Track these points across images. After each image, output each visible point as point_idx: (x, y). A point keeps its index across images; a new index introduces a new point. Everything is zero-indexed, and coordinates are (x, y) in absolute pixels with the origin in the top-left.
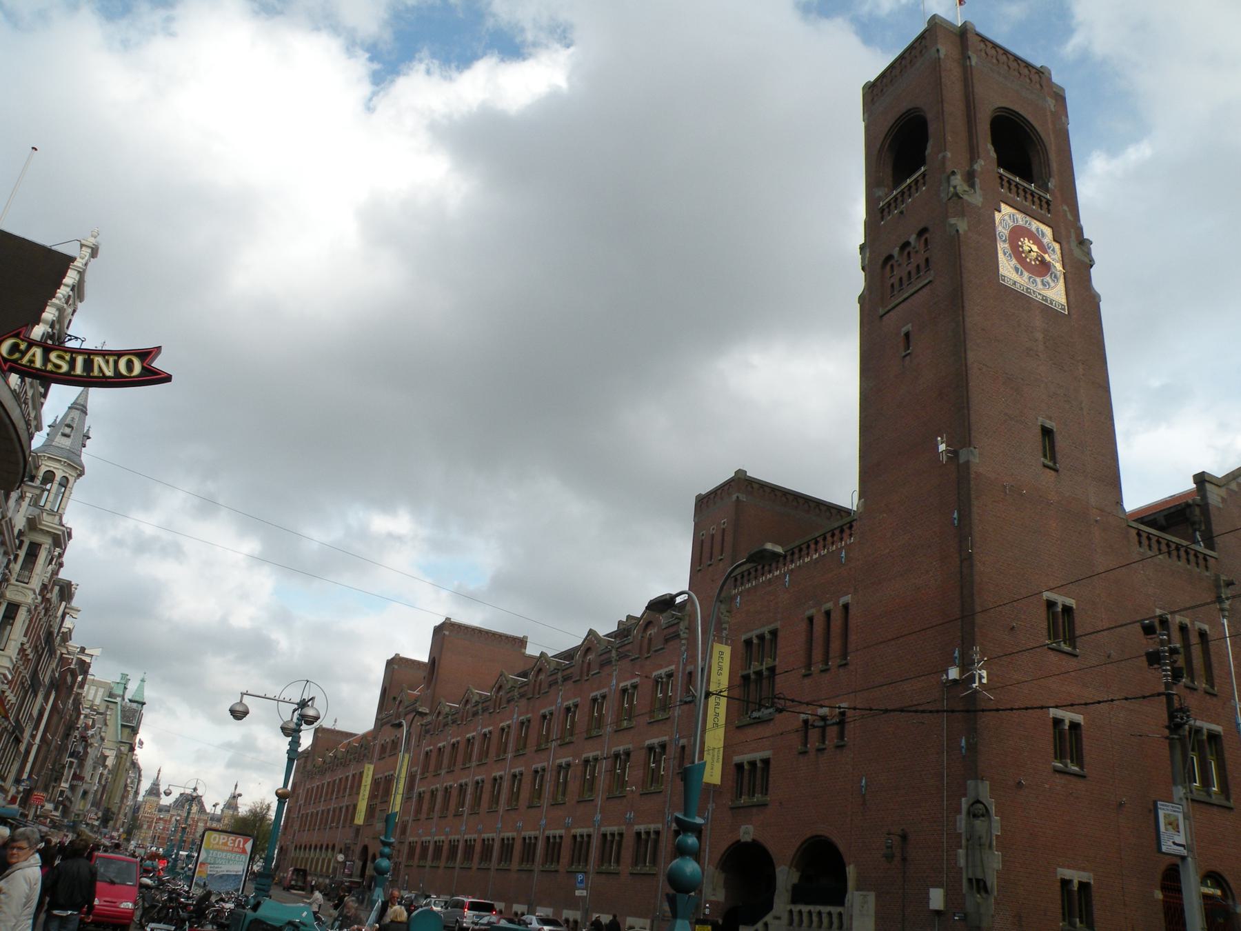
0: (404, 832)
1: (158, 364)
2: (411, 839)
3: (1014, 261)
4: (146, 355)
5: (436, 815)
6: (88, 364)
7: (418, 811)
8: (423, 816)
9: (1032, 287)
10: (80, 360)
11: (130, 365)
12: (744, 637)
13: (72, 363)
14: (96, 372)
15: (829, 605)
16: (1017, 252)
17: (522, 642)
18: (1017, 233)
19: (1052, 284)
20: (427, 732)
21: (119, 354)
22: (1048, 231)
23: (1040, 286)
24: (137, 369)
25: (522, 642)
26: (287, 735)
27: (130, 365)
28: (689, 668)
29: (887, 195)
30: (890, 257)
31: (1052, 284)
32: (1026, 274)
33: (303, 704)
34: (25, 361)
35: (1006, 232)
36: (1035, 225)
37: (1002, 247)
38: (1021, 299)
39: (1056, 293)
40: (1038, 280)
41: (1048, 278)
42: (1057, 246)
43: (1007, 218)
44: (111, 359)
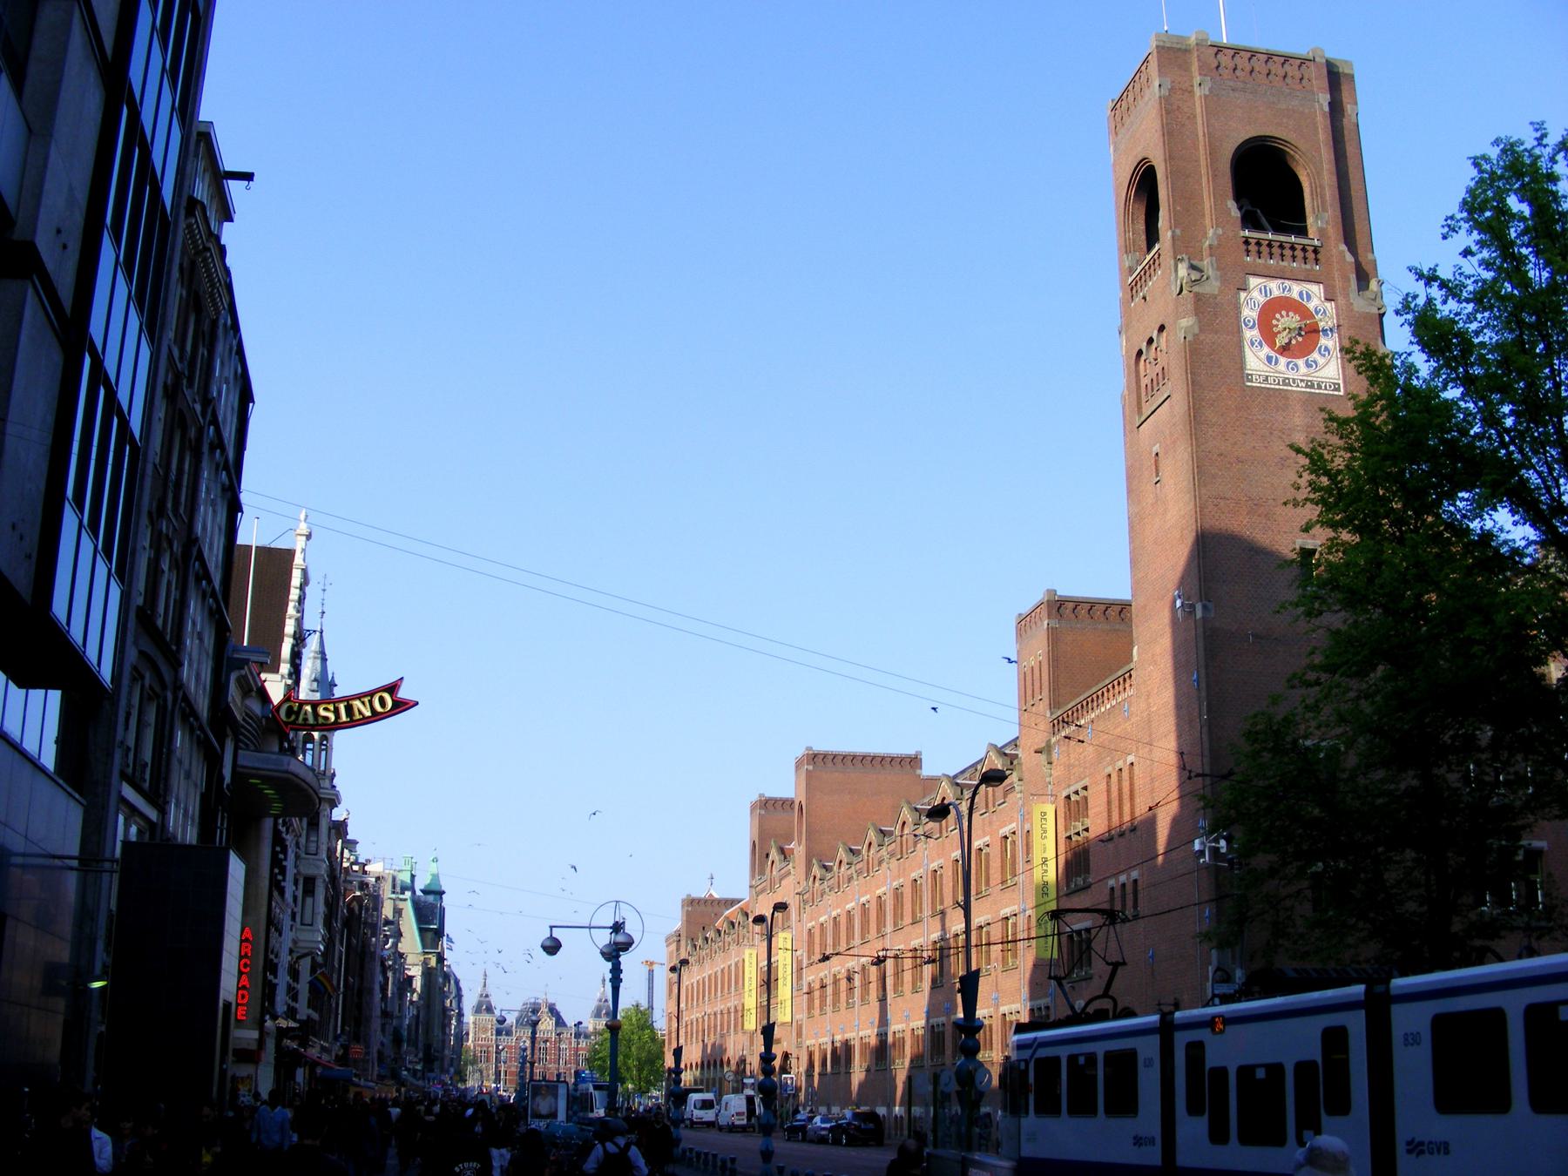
0: (799, 1035)
1: (403, 694)
2: (808, 1043)
3: (1266, 350)
4: (392, 689)
5: (829, 1009)
6: (349, 709)
7: (810, 1007)
8: (817, 1012)
9: (1291, 375)
10: (342, 707)
11: (382, 702)
12: (1065, 794)
13: (336, 712)
14: (358, 716)
15: (1120, 764)
16: (1268, 336)
17: (914, 761)
18: (1270, 310)
19: (1321, 361)
20: (805, 902)
21: (371, 694)
22: (1316, 290)
23: (1303, 369)
24: (389, 703)
25: (914, 761)
26: (608, 960)
27: (382, 702)
28: (1027, 827)
29: (1139, 262)
30: (1140, 353)
31: (1321, 361)
32: (1283, 360)
33: (617, 928)
34: (300, 720)
35: (1255, 315)
36: (1296, 290)
37: (1251, 334)
38: (1275, 398)
39: (1328, 370)
40: (1301, 362)
41: (1315, 355)
42: (1330, 306)
43: (1255, 294)
44: (366, 700)
